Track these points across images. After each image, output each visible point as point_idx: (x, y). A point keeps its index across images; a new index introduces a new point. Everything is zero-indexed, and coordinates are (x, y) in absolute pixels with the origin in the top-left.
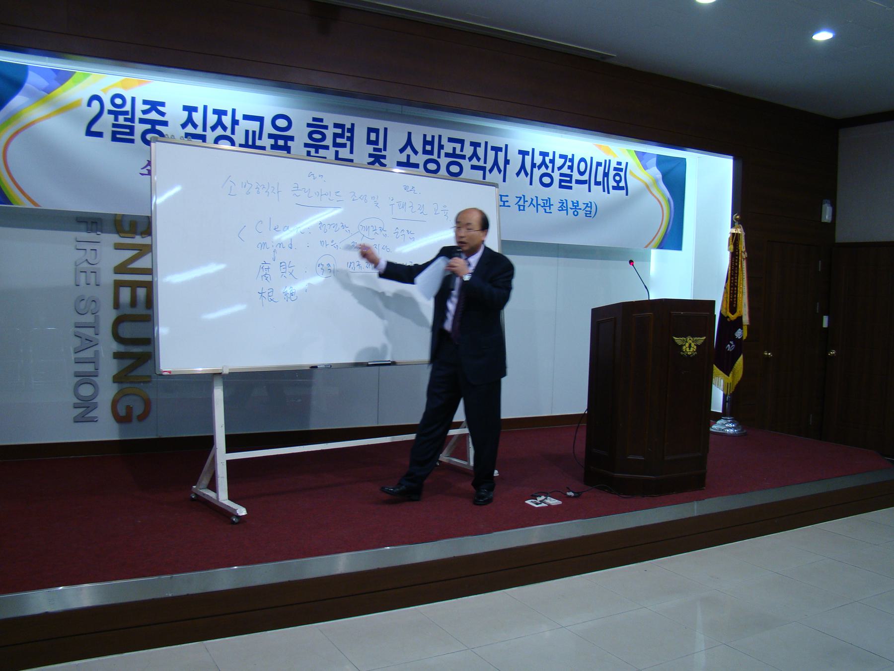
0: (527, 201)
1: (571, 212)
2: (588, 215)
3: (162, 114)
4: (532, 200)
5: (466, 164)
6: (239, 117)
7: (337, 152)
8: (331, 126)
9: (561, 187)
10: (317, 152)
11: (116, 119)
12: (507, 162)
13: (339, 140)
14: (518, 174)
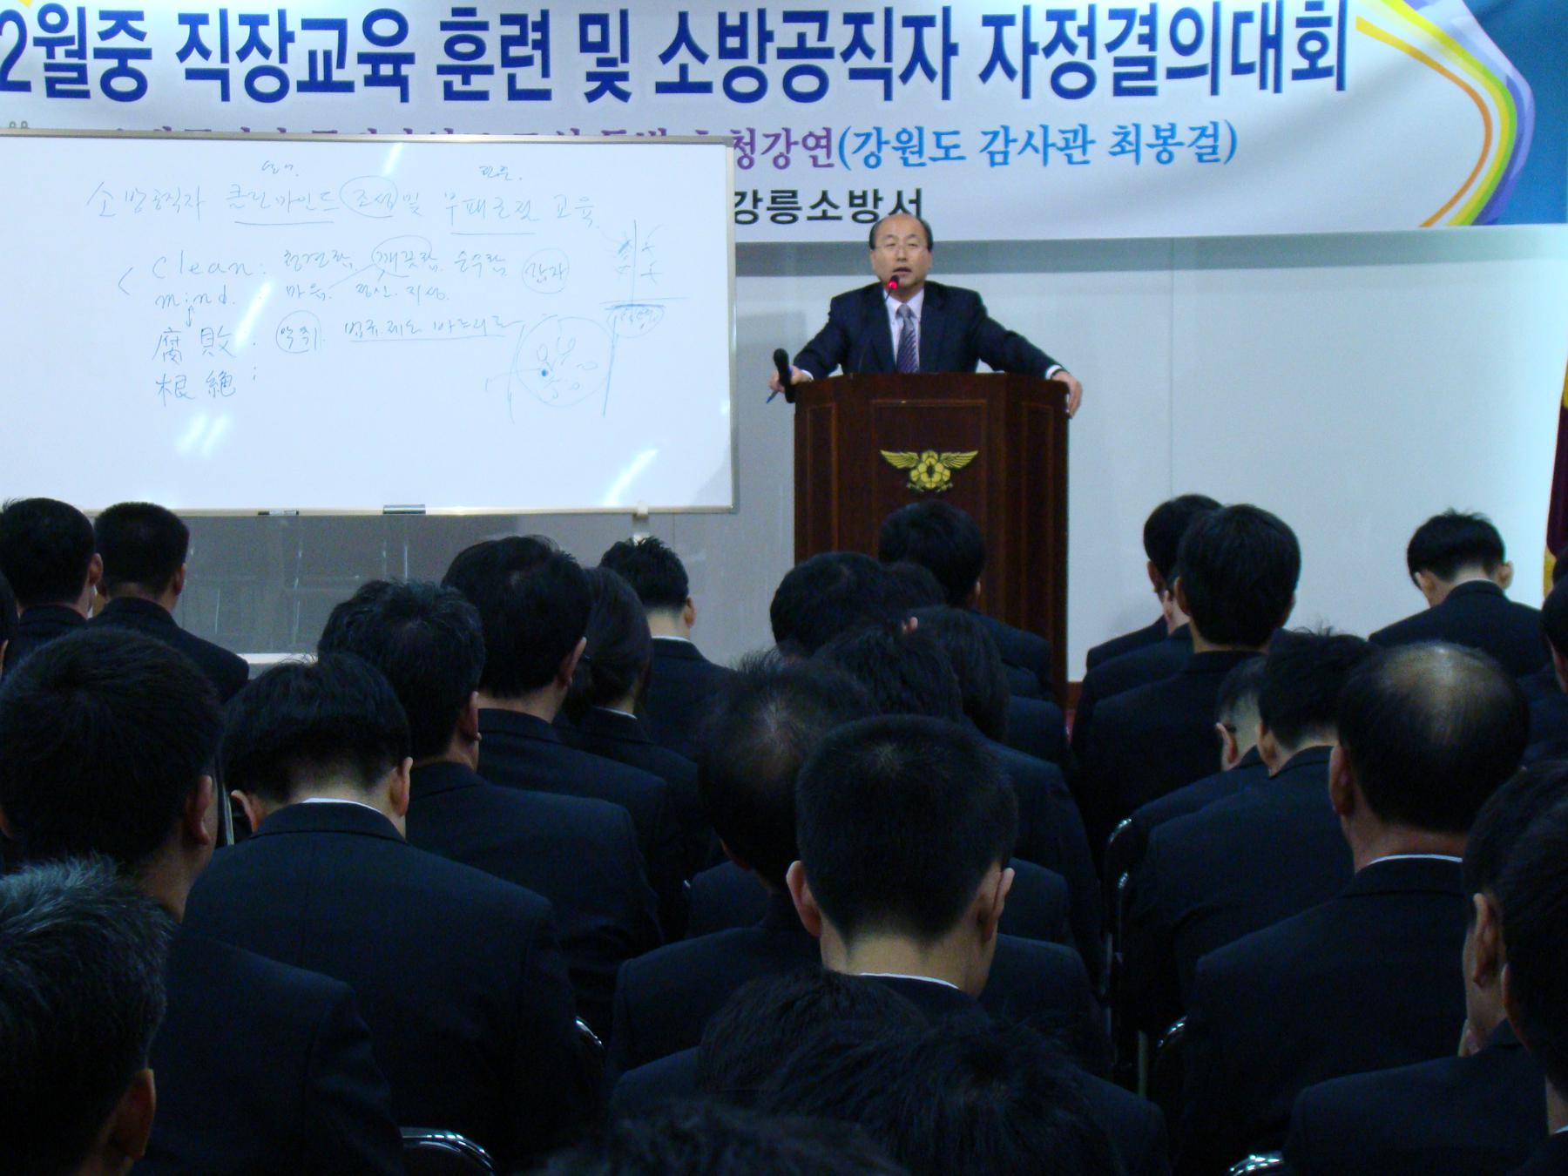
0: (1014, 141)
1: (1148, 155)
2: (1205, 158)
3: (140, 36)
4: (1031, 135)
5: (834, 68)
6: (293, 25)
7: (512, 79)
8: (494, 23)
9: (1119, 91)
10: (466, 81)
11: (51, 55)
12: (950, 49)
13: (515, 51)
14: (985, 75)
